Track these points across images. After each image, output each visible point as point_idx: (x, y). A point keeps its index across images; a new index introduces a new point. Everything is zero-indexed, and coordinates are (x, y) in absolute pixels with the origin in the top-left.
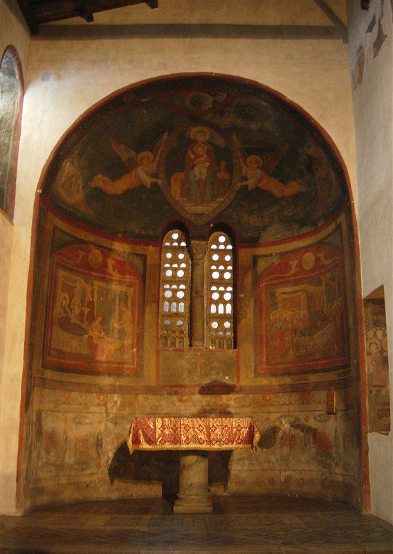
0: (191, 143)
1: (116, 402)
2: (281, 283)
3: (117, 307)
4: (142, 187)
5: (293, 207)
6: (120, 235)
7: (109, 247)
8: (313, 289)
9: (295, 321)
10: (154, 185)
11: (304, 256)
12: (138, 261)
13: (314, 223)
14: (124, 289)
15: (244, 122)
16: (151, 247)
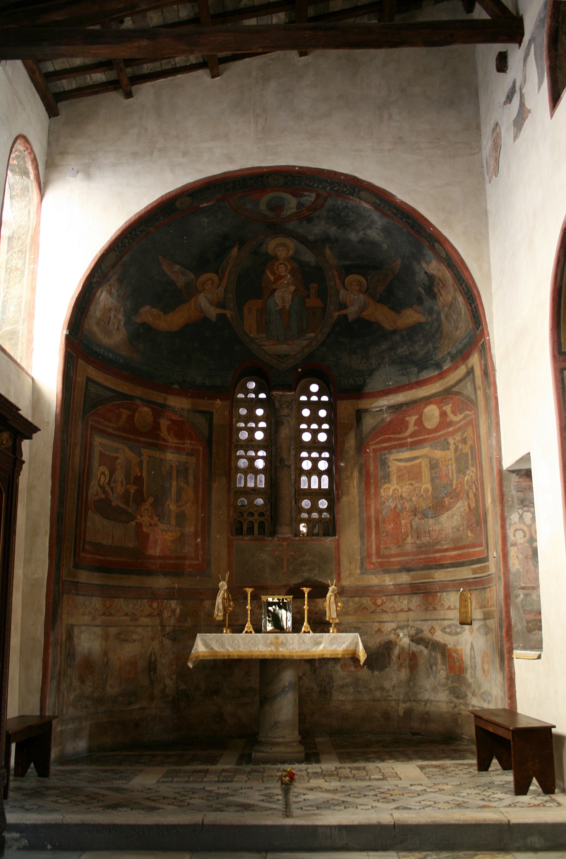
0: (272, 259)
1: (174, 611)
2: (395, 447)
3: (174, 483)
4: (205, 319)
5: (409, 343)
6: (176, 386)
7: (161, 401)
8: (438, 454)
9: (414, 499)
10: (221, 317)
11: (426, 410)
13: (438, 366)
14: (184, 458)
15: (340, 231)
16: (218, 401)
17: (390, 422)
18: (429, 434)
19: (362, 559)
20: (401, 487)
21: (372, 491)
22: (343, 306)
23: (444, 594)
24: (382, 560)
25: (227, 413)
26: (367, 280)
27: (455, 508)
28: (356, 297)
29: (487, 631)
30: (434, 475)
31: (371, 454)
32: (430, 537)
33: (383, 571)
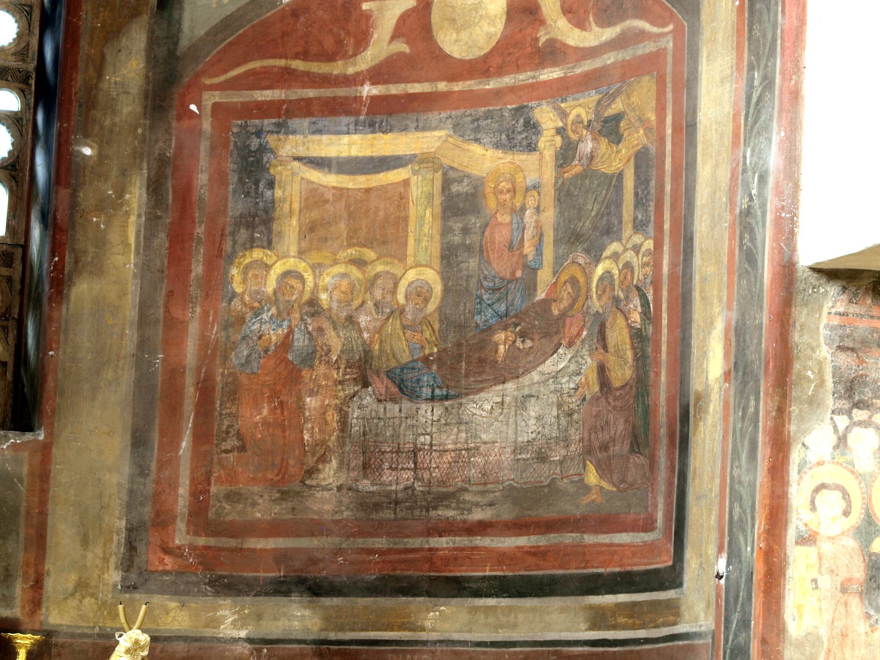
2: (305, 108)
9: (363, 320)
18: (452, 79)
19: (130, 530)
20: (317, 268)
21: (198, 269)
24: (212, 541)
27: (535, 376)
30: (457, 239)
32: (415, 469)
33: (211, 583)
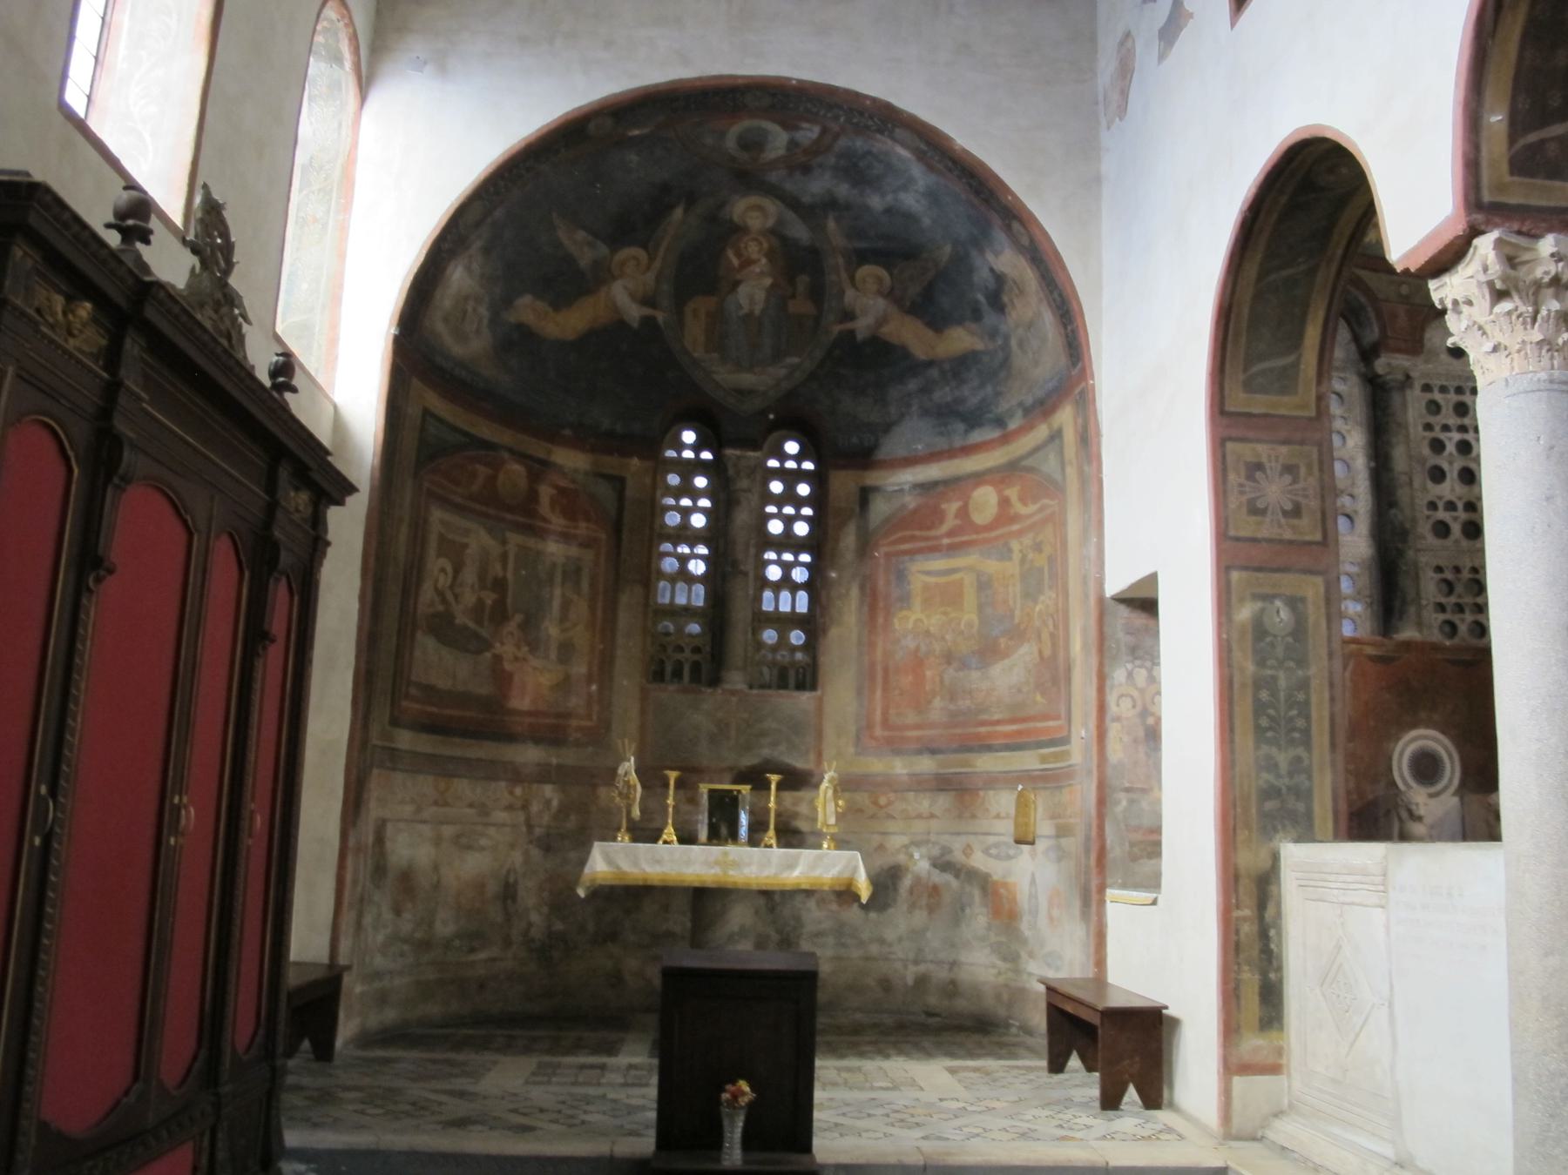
1: (548, 802)
3: (558, 592)
4: (621, 324)
6: (567, 432)
7: (541, 455)
8: (992, 566)
9: (948, 637)
10: (648, 322)
12: (604, 491)
13: (1000, 422)
14: (574, 551)
16: (635, 461)
17: (915, 511)
21: (880, 620)
22: (849, 316)
23: (991, 793)
25: (648, 481)
26: (891, 275)
28: (871, 302)
29: (1061, 855)
31: (882, 561)
